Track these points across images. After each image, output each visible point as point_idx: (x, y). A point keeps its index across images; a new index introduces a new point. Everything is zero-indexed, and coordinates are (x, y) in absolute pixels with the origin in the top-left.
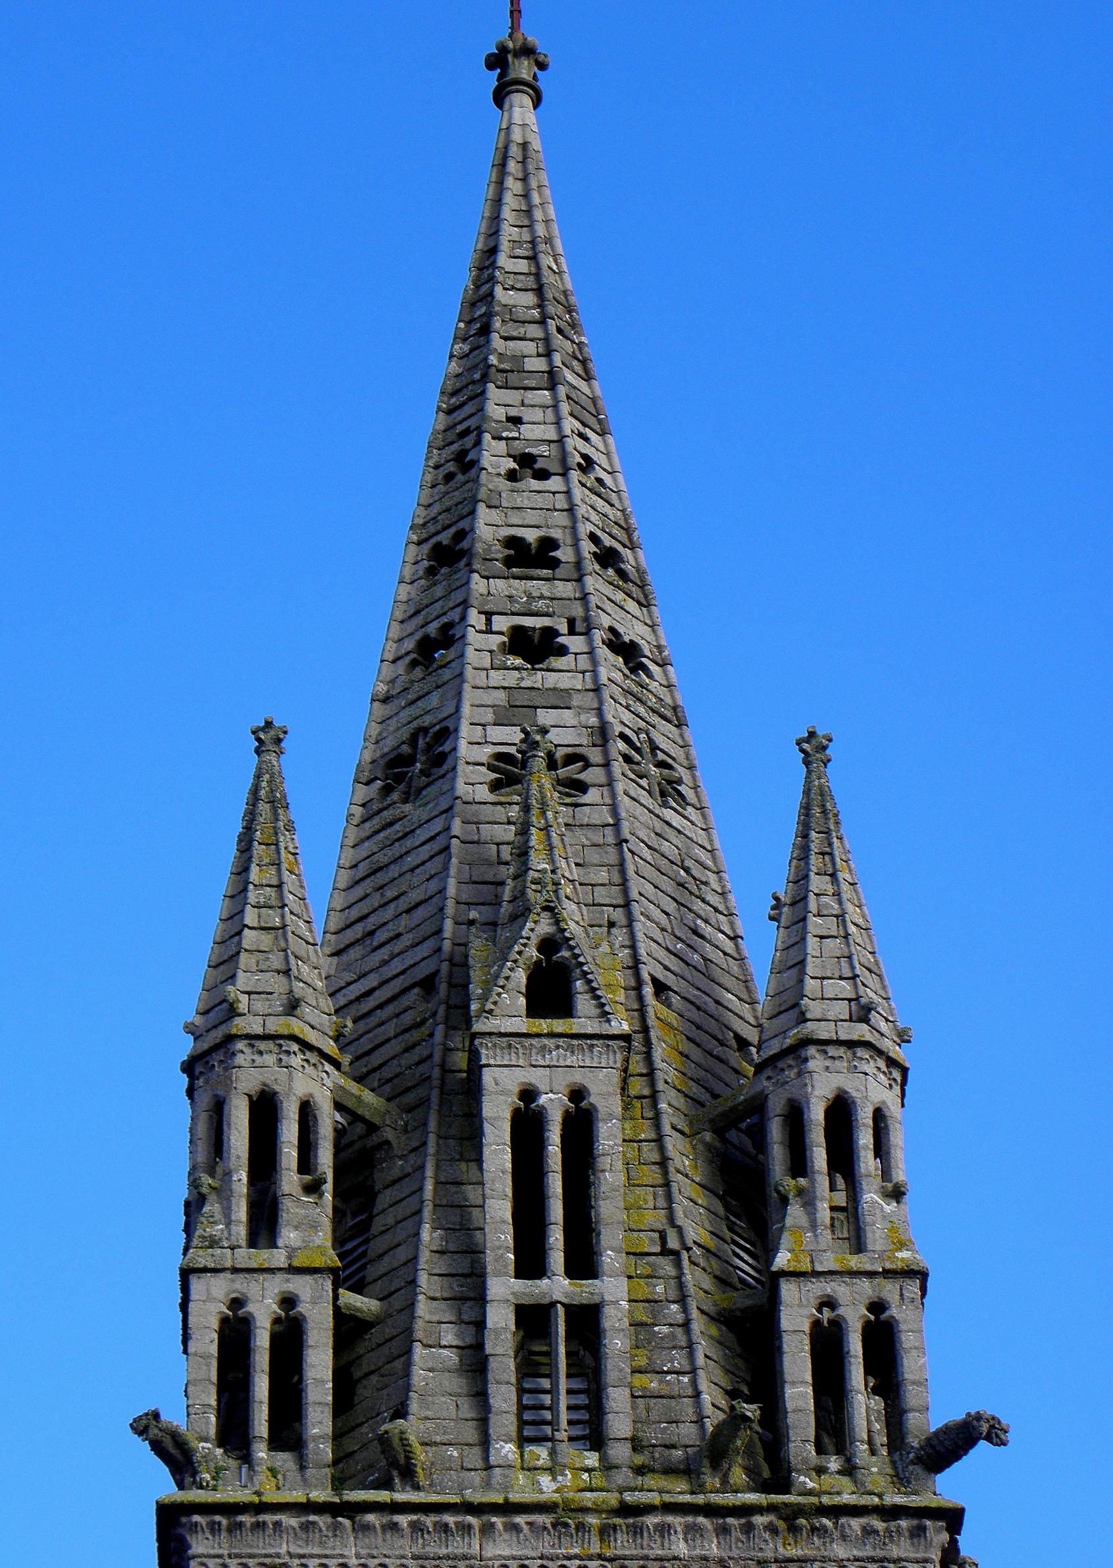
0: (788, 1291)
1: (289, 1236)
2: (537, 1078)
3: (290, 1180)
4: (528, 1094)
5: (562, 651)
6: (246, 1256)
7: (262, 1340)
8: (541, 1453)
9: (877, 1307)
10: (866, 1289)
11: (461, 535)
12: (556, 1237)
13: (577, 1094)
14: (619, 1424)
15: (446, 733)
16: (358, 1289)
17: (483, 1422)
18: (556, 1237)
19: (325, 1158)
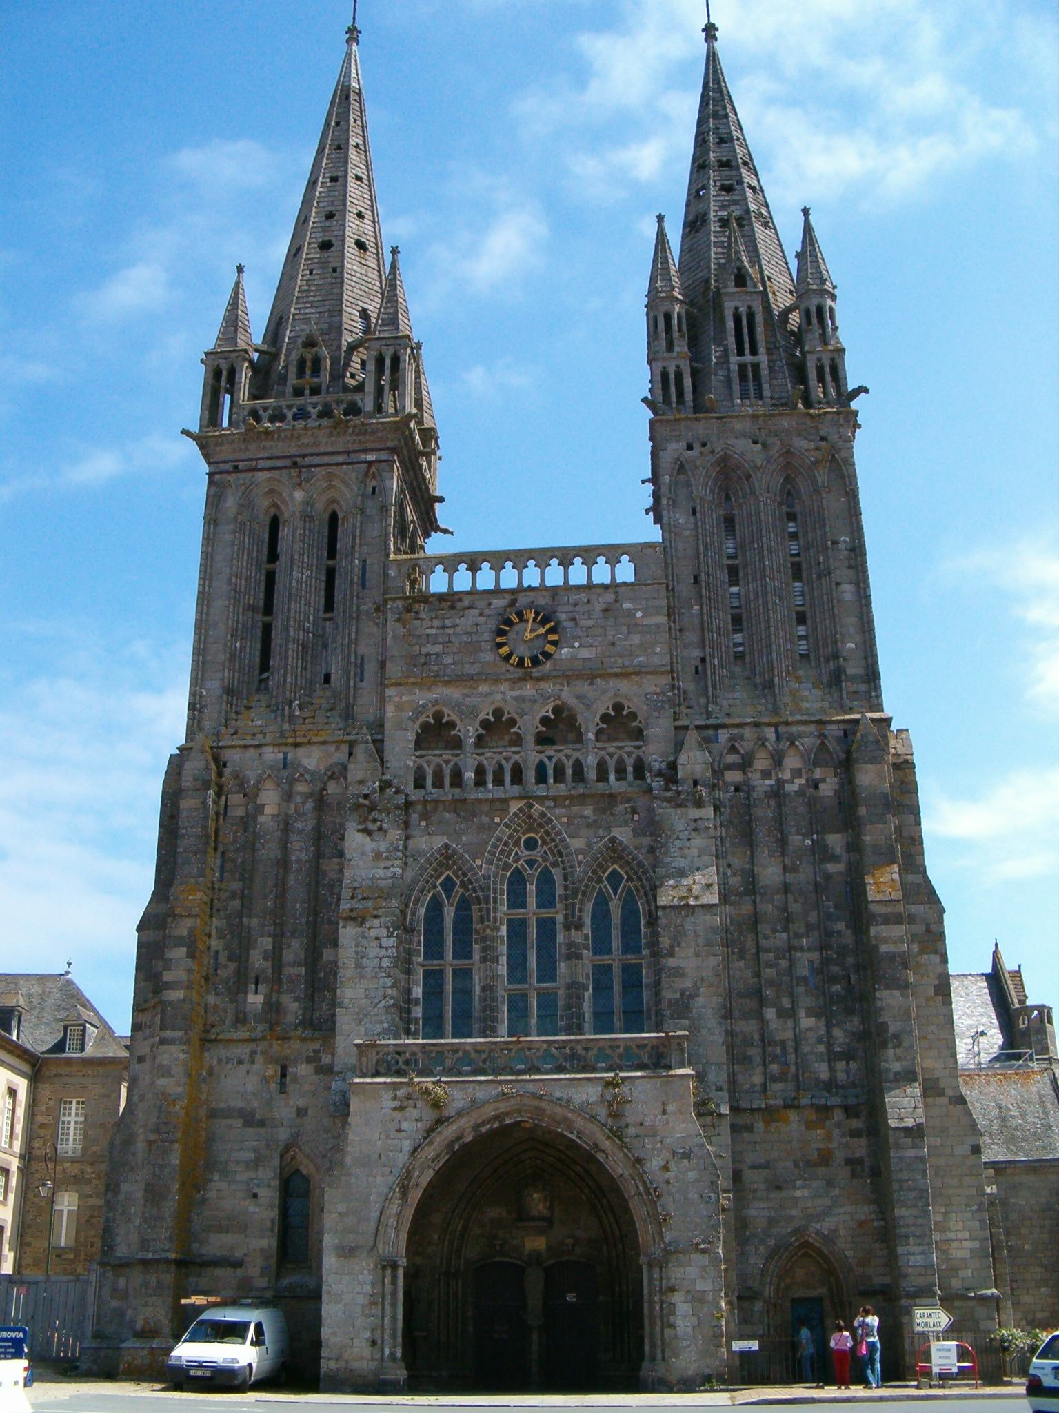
0: (809, 356)
1: (677, 349)
2: (738, 304)
3: (676, 334)
4: (737, 309)
5: (735, 190)
6: (666, 355)
7: (672, 376)
8: (748, 402)
9: (832, 360)
11: (705, 160)
12: (747, 345)
13: (749, 307)
14: (767, 393)
15: (706, 213)
16: (696, 362)
17: (731, 395)
18: (747, 345)
19: (684, 328)
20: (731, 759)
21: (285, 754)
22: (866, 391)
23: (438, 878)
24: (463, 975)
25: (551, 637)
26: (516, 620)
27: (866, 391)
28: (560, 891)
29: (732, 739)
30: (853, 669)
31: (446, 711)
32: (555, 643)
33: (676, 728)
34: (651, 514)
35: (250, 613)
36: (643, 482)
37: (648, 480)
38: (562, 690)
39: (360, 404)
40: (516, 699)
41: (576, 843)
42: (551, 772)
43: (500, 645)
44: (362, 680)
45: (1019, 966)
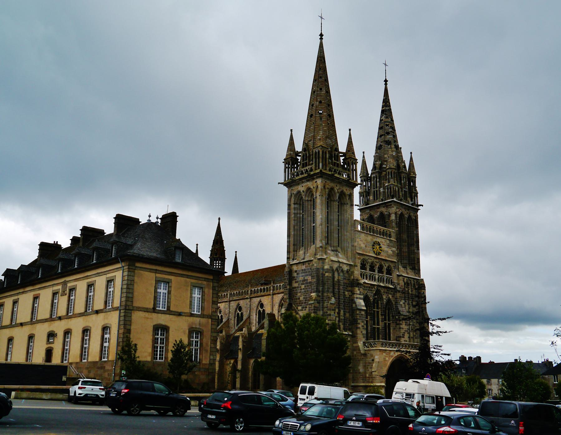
25: (381, 249)
29: (403, 279)
30: (417, 268)
32: (381, 250)
41: (384, 297)
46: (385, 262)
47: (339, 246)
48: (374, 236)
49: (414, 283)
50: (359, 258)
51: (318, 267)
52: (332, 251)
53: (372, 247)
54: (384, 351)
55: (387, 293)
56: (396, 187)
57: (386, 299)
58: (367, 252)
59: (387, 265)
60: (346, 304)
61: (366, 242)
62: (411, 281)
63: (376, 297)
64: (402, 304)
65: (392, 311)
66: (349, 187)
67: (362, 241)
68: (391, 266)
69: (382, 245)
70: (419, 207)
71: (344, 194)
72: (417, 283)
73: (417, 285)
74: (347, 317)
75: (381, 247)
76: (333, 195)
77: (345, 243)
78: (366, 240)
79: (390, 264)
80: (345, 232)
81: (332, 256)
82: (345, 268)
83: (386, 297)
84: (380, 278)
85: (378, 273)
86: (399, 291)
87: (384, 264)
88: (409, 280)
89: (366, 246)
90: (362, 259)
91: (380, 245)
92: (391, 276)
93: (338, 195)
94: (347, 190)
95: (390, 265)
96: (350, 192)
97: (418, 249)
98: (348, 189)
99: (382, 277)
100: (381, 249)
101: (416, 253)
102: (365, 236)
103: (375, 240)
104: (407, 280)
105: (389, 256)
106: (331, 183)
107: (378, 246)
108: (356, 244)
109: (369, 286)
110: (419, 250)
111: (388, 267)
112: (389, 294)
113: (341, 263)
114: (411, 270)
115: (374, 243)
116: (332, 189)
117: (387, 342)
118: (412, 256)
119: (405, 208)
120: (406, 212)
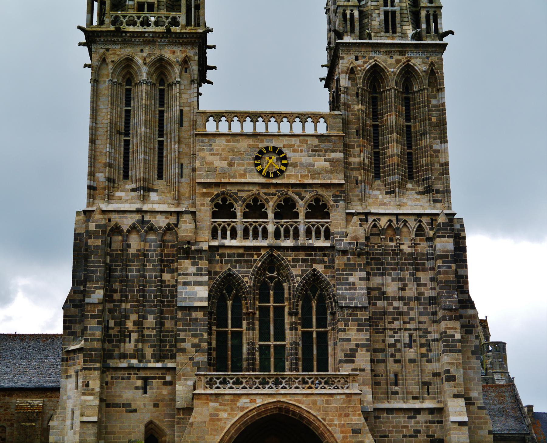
7: (348, 16)
9: (435, 12)
10: (433, 9)
20: (375, 231)
21: (143, 217)
22: (452, 33)
23: (224, 286)
24: (238, 336)
25: (284, 162)
26: (265, 152)
27: (452, 33)
28: (286, 295)
31: (228, 198)
32: (286, 165)
33: (347, 214)
34: (324, 82)
35: (118, 135)
36: (323, 66)
37: (326, 66)
38: (289, 190)
39: (178, 19)
40: (266, 194)
41: (296, 272)
42: (282, 232)
43: (257, 165)
44: (182, 177)
45: (486, 317)
46: (298, 190)
47: (160, 177)
48: (259, 137)
49: (420, 226)
50: (204, 195)
51: (80, 232)
52: (133, 190)
53: (252, 161)
54: (214, 397)
55: (304, 261)
56: (352, 10)
57: (300, 276)
58: (231, 177)
59: (308, 196)
60: (164, 302)
61: (231, 154)
62: (405, 222)
63: (275, 274)
64: (357, 281)
65: (331, 302)
66: (180, 44)
67: (218, 154)
68: (323, 197)
69: (287, 152)
70: (446, 40)
71: (169, 63)
72: (431, 224)
73: (432, 229)
74: (168, 328)
75: (285, 158)
76: (136, 73)
77: (173, 168)
78: (232, 151)
79: (320, 191)
80: (173, 143)
81: (126, 201)
82: (161, 222)
83: (303, 271)
84: (282, 230)
85: (275, 218)
86: (344, 252)
87: (297, 194)
88: (398, 221)
89: (231, 164)
90: (217, 196)
91: (281, 152)
92: (329, 219)
93: (144, 70)
94: (174, 53)
95: (320, 195)
96: (184, 55)
97: (443, 138)
98: (177, 49)
99: (291, 225)
100: (284, 162)
101: (438, 151)
102: (228, 141)
103: (261, 146)
104: (390, 221)
105: (316, 174)
106: (126, 47)
107: (274, 158)
108: (198, 164)
109: (241, 251)
110: (446, 142)
111: (317, 200)
112: (313, 261)
113: (148, 214)
114: (418, 197)
115: (261, 152)
116: (129, 62)
117: (228, 375)
118: (423, 161)
119: (387, 53)
120: (393, 61)
